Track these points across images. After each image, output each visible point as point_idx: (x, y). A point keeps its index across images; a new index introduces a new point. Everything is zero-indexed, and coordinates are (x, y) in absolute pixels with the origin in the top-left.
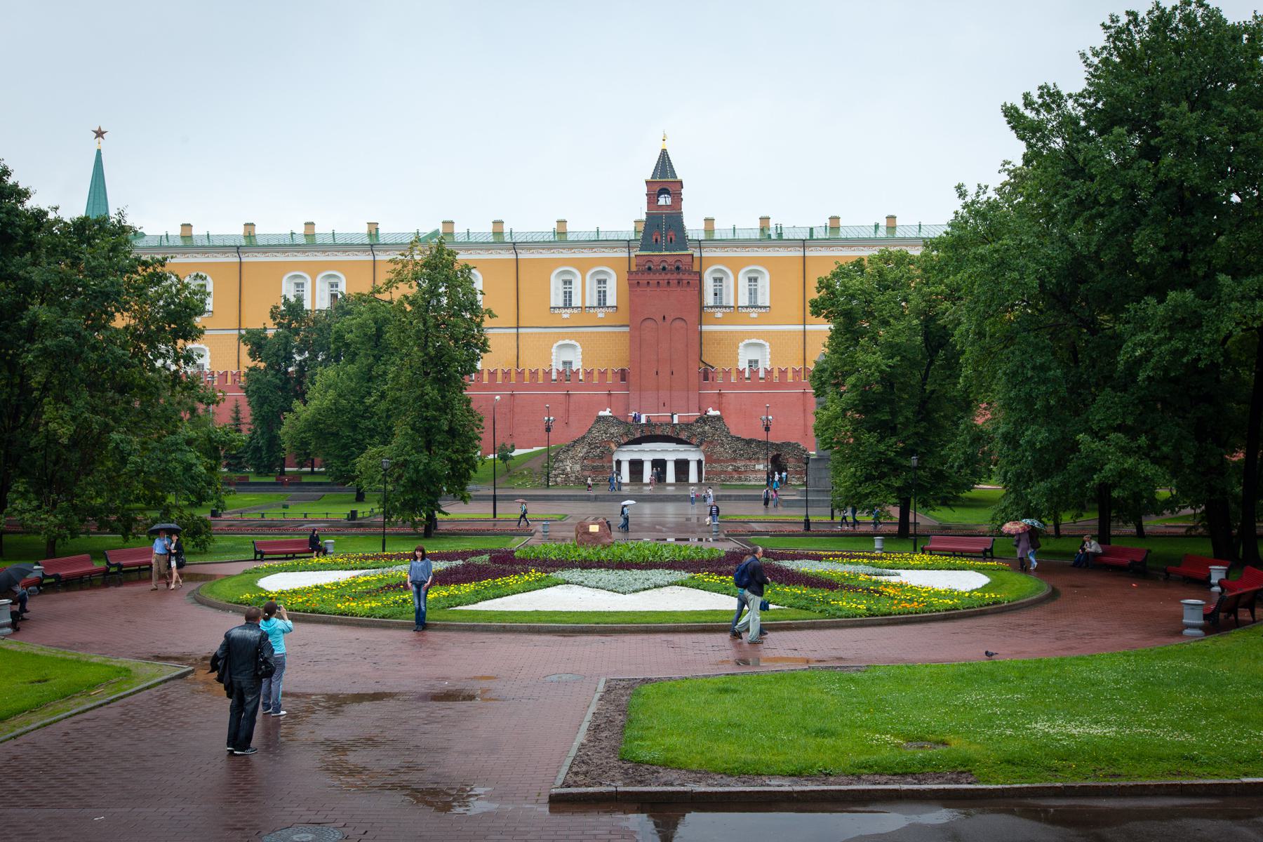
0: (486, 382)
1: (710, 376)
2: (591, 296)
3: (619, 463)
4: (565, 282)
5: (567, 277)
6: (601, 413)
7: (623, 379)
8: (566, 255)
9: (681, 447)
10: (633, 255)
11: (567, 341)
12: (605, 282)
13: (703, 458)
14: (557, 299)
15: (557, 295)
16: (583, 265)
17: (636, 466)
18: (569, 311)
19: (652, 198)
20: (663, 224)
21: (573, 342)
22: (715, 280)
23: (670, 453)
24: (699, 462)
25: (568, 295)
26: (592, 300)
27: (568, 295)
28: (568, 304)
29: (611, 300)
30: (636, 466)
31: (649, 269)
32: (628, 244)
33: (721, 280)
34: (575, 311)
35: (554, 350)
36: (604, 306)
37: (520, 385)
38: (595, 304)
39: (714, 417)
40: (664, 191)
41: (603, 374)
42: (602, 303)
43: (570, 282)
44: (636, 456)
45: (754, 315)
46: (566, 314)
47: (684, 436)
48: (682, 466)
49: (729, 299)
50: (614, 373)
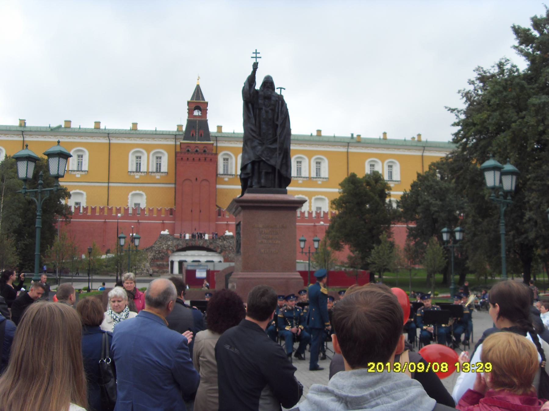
0: (106, 214)
1: (222, 214)
2: (153, 166)
3: (172, 262)
4: (137, 157)
5: (139, 155)
6: (163, 232)
7: (171, 214)
8: (139, 141)
9: (210, 254)
10: (178, 143)
11: (138, 192)
12: (160, 158)
14: (132, 167)
15: (132, 164)
16: (149, 148)
18: (139, 174)
19: (190, 112)
20: (197, 126)
21: (141, 192)
22: (224, 159)
25: (139, 165)
26: (153, 168)
28: (138, 170)
29: (164, 168)
31: (188, 151)
32: (175, 136)
33: (227, 159)
34: (143, 174)
35: (130, 196)
36: (160, 172)
37: (110, 216)
38: (155, 170)
39: (229, 236)
40: (198, 108)
41: (159, 211)
42: (158, 170)
43: (140, 158)
44: (182, 259)
46: (137, 176)
47: (212, 247)
50: (166, 210)
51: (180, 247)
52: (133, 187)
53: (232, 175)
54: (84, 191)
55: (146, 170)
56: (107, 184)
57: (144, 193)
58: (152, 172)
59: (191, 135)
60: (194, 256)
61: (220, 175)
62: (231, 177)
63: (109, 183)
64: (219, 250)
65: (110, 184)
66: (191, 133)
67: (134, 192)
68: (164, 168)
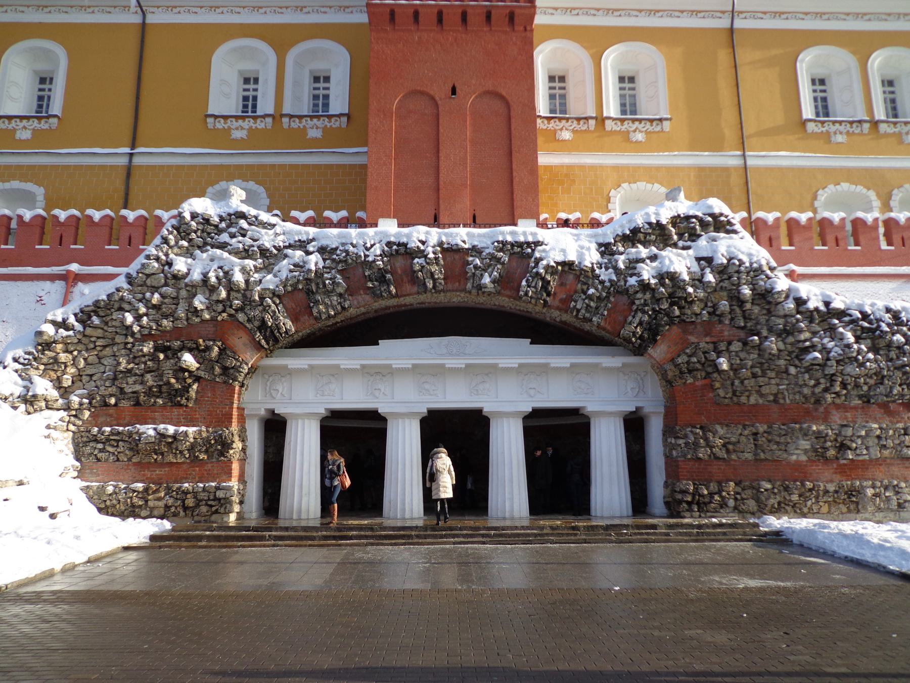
3: (275, 428)
18: (247, 124)
22: (552, 79)
23: (506, 383)
24: (634, 426)
26: (298, 100)
30: (355, 439)
34: (260, 125)
44: (353, 397)
48: (557, 441)
49: (580, 102)
52: (222, 167)
53: (587, 119)
54: (39, 184)
55: (270, 110)
58: (291, 116)
60: (439, 371)
64: (634, 328)
68: (339, 103)
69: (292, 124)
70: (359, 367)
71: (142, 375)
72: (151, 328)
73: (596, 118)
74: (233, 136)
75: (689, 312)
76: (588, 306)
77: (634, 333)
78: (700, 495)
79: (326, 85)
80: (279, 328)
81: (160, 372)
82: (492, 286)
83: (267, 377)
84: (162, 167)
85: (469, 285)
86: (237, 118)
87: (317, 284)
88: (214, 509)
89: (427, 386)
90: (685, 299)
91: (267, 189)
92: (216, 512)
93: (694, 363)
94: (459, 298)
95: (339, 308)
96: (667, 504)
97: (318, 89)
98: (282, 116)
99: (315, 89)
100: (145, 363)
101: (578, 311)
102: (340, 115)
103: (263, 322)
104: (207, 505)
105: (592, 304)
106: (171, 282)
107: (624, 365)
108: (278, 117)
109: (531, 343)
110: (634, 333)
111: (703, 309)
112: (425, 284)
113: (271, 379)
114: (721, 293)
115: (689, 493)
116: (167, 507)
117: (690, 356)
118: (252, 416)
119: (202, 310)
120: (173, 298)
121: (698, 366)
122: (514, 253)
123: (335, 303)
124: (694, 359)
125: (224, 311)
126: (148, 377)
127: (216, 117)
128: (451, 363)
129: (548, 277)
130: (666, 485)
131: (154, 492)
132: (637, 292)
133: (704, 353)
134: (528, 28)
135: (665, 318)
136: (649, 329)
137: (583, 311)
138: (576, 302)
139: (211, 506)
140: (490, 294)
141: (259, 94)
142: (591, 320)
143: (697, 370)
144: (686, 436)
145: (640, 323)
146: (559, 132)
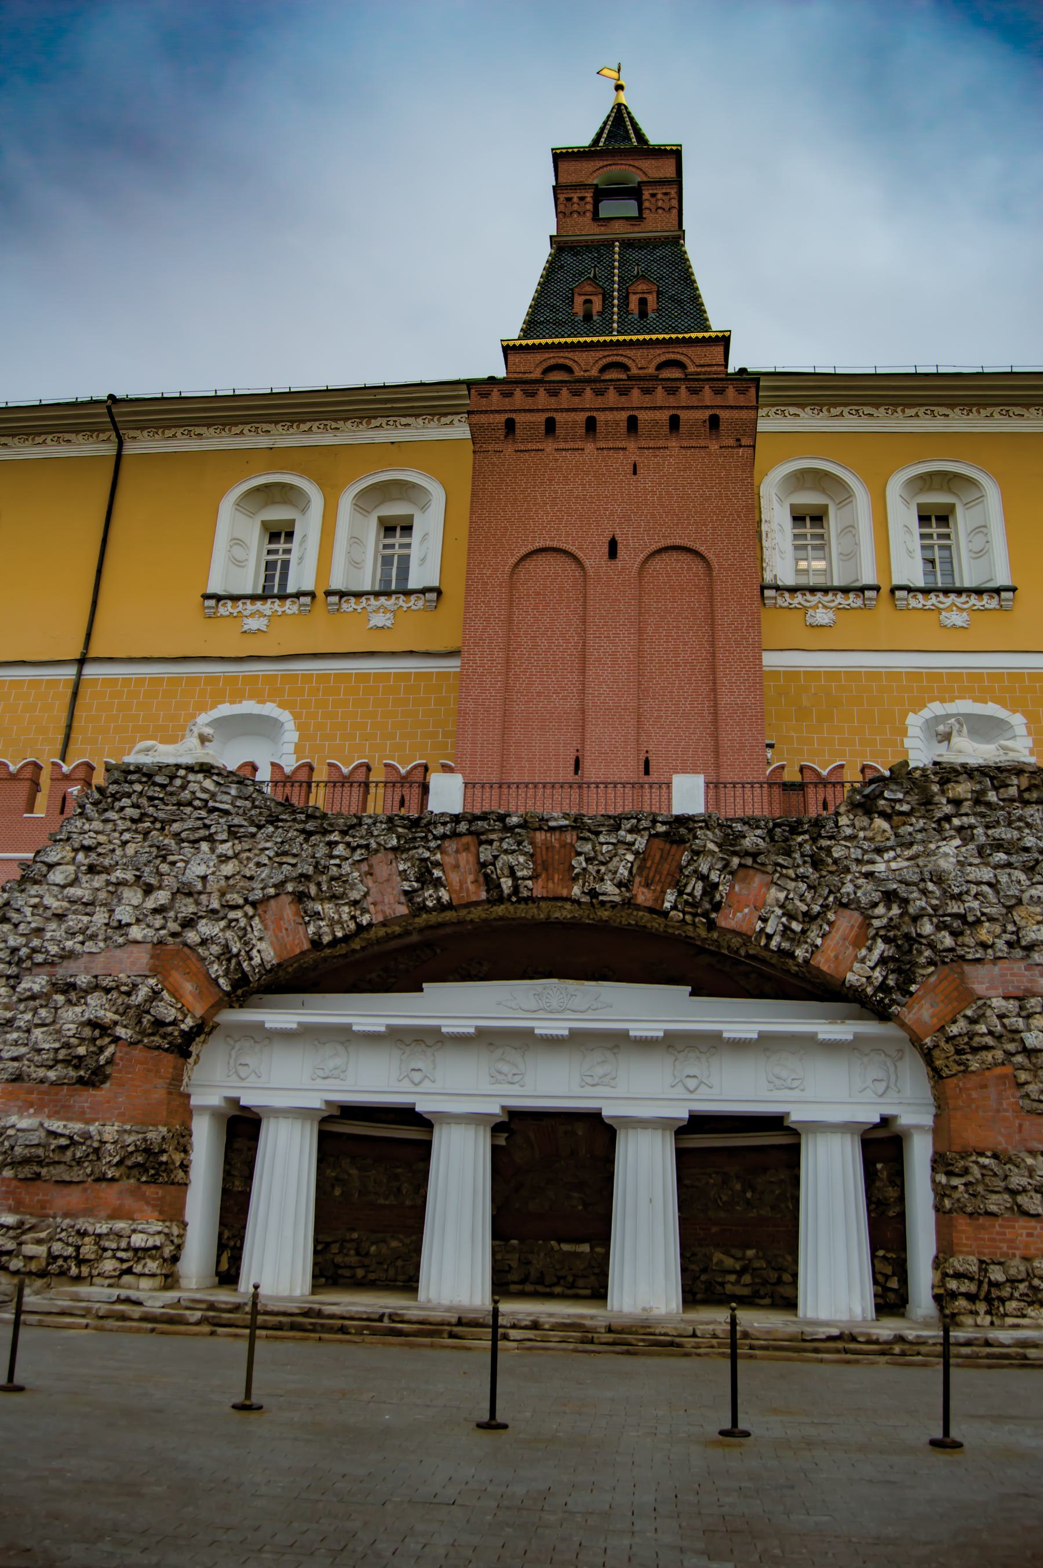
2: (355, 564)
9: (740, 1019)
11: (249, 707)
12: (407, 529)
13: (913, 1111)
17: (372, 1167)
18: (267, 607)
21: (270, 709)
24: (881, 1150)
25: (275, 571)
27: (275, 571)
29: (423, 573)
34: (290, 607)
42: (393, 587)
45: (957, 619)
48: (738, 1178)
51: (333, 919)
55: (308, 585)
56: (71, 671)
57: (285, 716)
59: (579, 307)
61: (778, 588)
62: (853, 600)
63: (82, 662)
65: (89, 670)
66: (579, 300)
67: (225, 709)
69: (344, 606)
70: (383, 1029)
71: (28, 1031)
72: (47, 952)
73: (877, 589)
74: (246, 628)
75: (968, 940)
76: (787, 928)
77: (868, 978)
78: (990, 1282)
79: (405, 540)
80: (251, 959)
81: (58, 1026)
82: (617, 891)
83: (232, 1043)
84: (127, 681)
85: (576, 891)
86: (253, 598)
87: (319, 884)
88: (125, 1266)
89: (505, 1068)
90: (962, 917)
91: (296, 716)
92: (129, 1271)
93: (982, 1035)
94: (565, 913)
95: (352, 926)
96: (937, 1298)
97: (392, 546)
98: (329, 593)
99: (385, 547)
100: (35, 1011)
101: (769, 937)
102: (424, 591)
103: (226, 947)
104: (114, 1257)
105: (796, 926)
106: (84, 878)
107: (857, 1037)
108: (320, 595)
109: (692, 994)
110: (868, 978)
111: (998, 937)
112: (499, 886)
113: (237, 1046)
114: (1031, 909)
115: (971, 1279)
116: (52, 1258)
117: (973, 1021)
118: (203, 1109)
119: (129, 925)
120: (86, 904)
121: (989, 1040)
122: (657, 835)
123: (345, 917)
124: (982, 1028)
125: (163, 928)
126: (37, 1033)
127: (218, 598)
128: (544, 1028)
129: (714, 877)
130: (937, 1264)
131: (32, 1229)
132: (875, 905)
133: (1001, 1017)
134: (744, 441)
135: (928, 953)
136: (898, 971)
137: (777, 939)
138: (765, 920)
139: (122, 1261)
140: (614, 905)
141: (293, 558)
142: (791, 955)
143: (987, 1048)
144: (966, 1171)
145: (883, 961)
146: (811, 612)
